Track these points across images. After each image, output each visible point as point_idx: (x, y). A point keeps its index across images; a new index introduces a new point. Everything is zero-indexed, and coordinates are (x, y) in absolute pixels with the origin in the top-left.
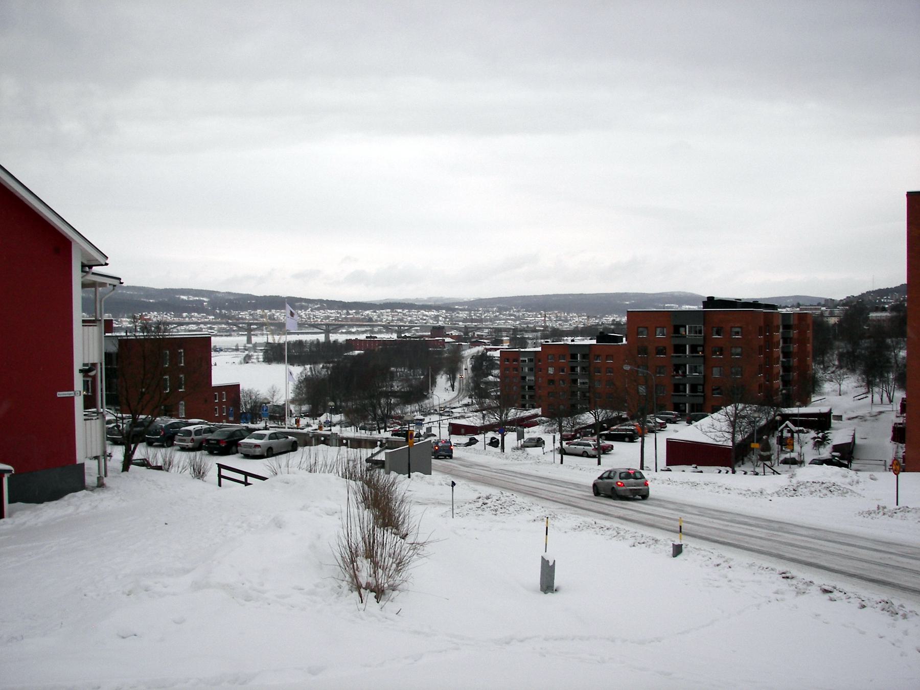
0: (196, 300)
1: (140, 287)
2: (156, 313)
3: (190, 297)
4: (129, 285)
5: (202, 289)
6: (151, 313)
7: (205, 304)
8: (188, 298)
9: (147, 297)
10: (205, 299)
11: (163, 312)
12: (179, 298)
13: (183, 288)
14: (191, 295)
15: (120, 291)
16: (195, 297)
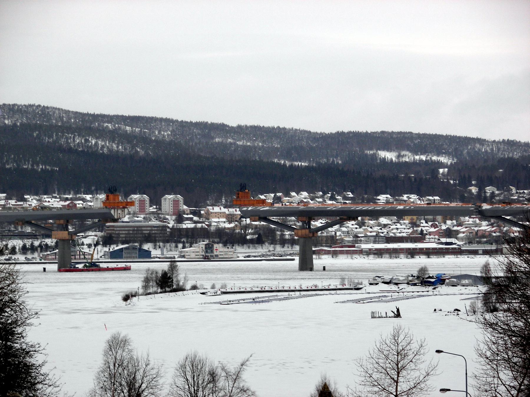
0: (421, 161)
1: (273, 128)
2: (305, 194)
3: (403, 153)
4: (243, 124)
5: (439, 132)
6: (293, 194)
7: (441, 171)
8: (399, 156)
9: (288, 155)
10: (443, 159)
11: (325, 193)
12: (374, 156)
13: (389, 129)
14: (409, 149)
15: (217, 140)
16: (416, 153)
